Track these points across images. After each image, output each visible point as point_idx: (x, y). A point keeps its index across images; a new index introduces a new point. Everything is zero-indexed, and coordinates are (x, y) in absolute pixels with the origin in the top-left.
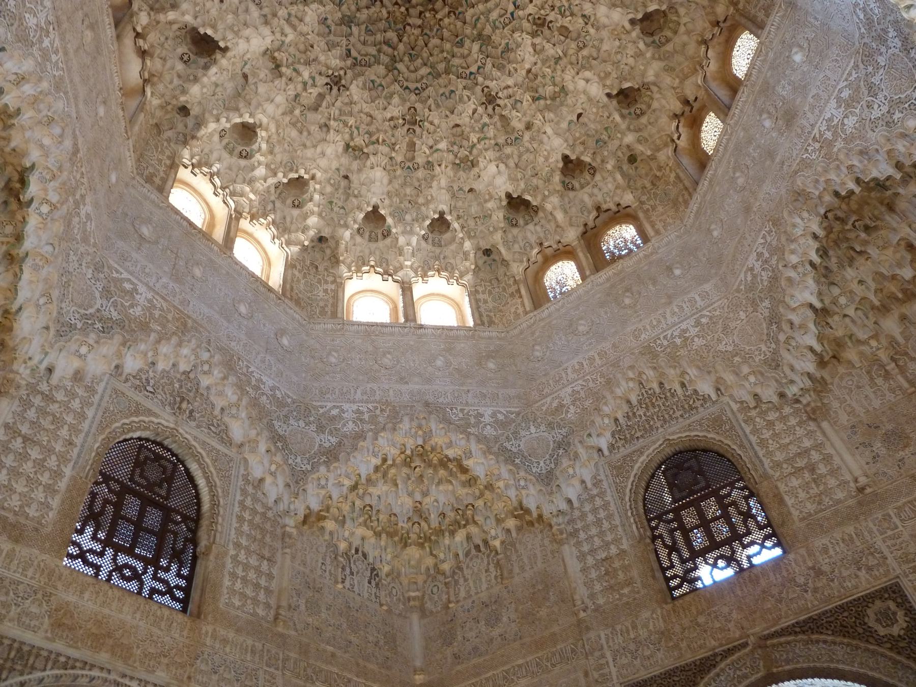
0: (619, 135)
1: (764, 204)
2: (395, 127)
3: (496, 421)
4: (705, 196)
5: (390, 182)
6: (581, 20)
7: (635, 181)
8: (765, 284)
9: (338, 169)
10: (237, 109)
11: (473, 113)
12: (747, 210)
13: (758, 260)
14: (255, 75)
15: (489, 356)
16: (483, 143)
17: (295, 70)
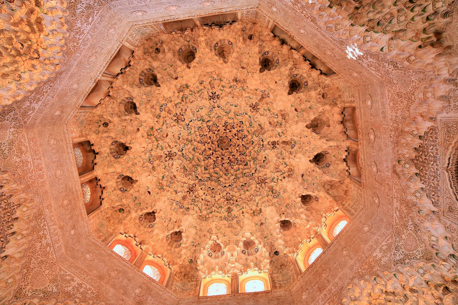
0: (136, 209)
1: (104, 288)
2: (182, 110)
3: (29, 110)
4: (104, 250)
5: (164, 97)
6: (187, 206)
7: (111, 210)
8: (66, 289)
9: (182, 77)
10: (237, 58)
11: (169, 145)
12: (101, 278)
13: (78, 284)
14: (241, 72)
15: (62, 112)
16: (156, 145)
17: (231, 87)
